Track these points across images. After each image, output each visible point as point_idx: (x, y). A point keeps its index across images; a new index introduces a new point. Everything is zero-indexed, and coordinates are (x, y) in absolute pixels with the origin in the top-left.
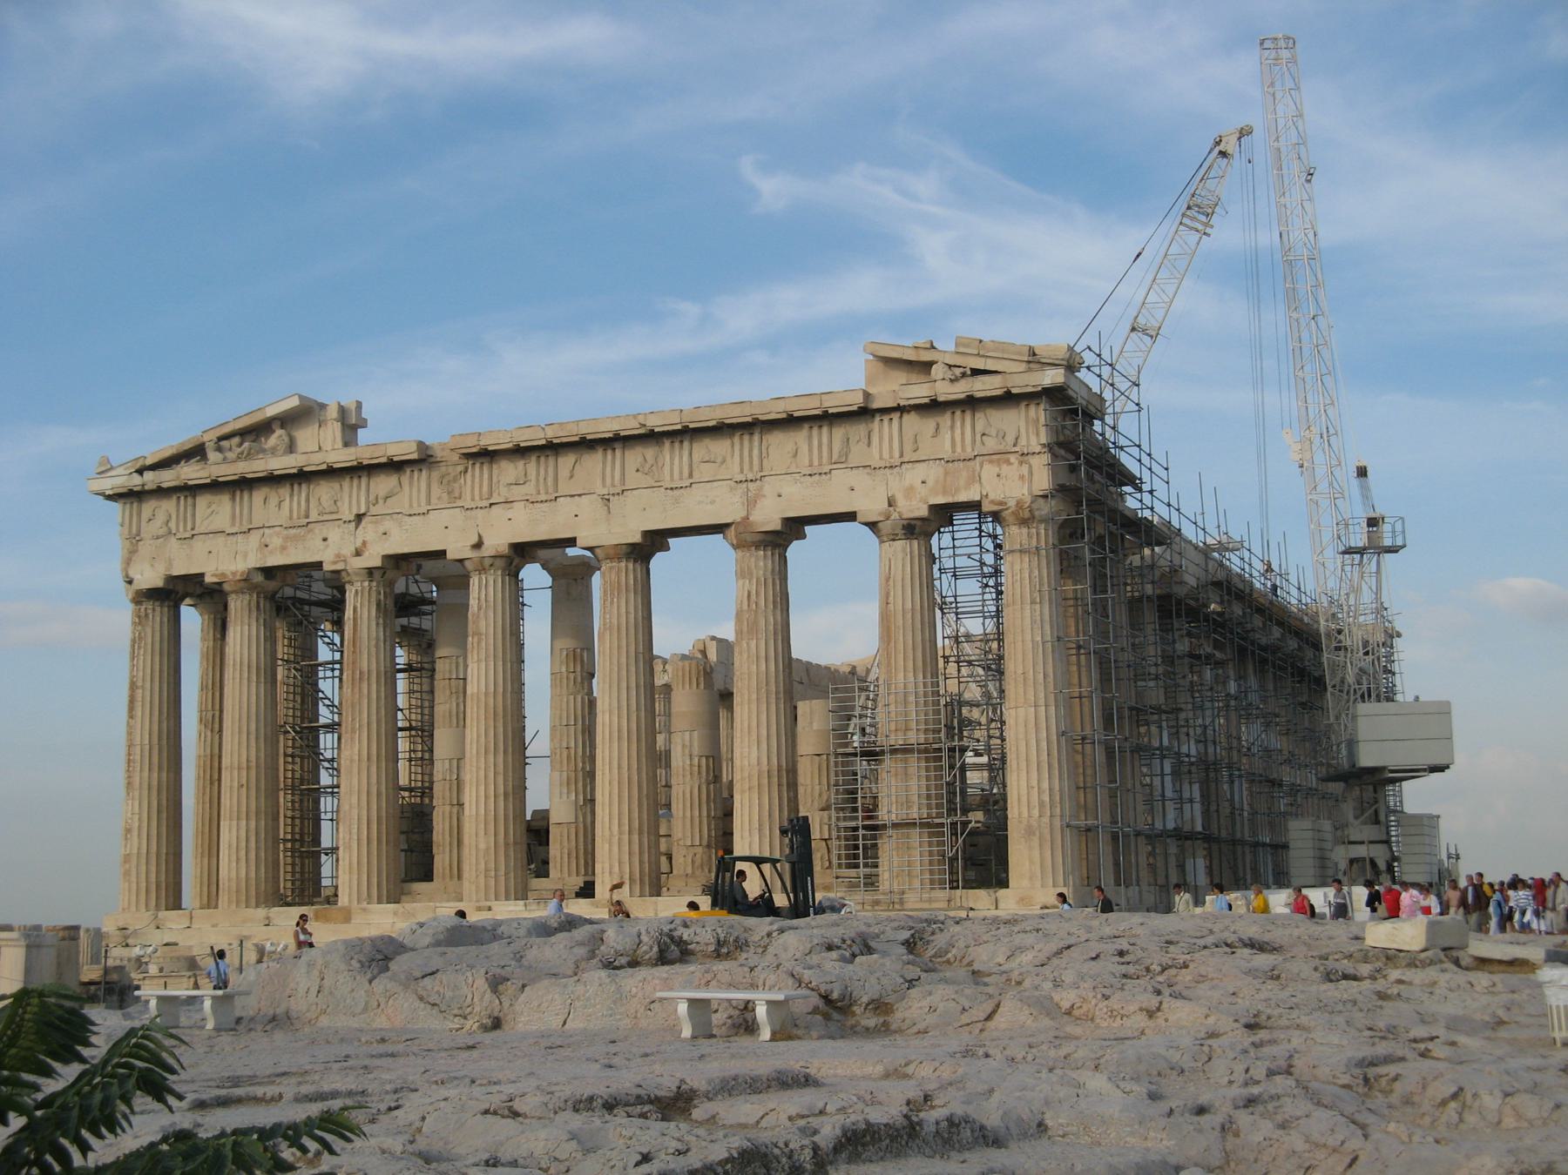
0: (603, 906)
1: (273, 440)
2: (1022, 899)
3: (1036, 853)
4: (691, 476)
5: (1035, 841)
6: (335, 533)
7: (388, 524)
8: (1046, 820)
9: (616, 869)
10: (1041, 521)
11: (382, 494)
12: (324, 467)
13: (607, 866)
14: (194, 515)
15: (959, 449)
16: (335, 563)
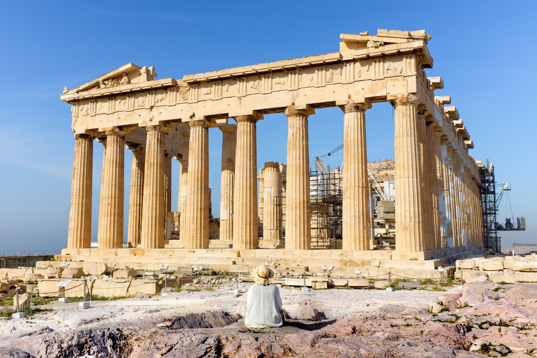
0: (235, 252)
1: (123, 80)
2: (402, 256)
3: (408, 237)
4: (272, 89)
5: (408, 231)
6: (143, 113)
7: (161, 109)
8: (412, 223)
9: (240, 238)
10: (412, 103)
11: (160, 99)
12: (139, 89)
13: (237, 237)
14: (96, 108)
15: (377, 75)
16: (143, 124)
